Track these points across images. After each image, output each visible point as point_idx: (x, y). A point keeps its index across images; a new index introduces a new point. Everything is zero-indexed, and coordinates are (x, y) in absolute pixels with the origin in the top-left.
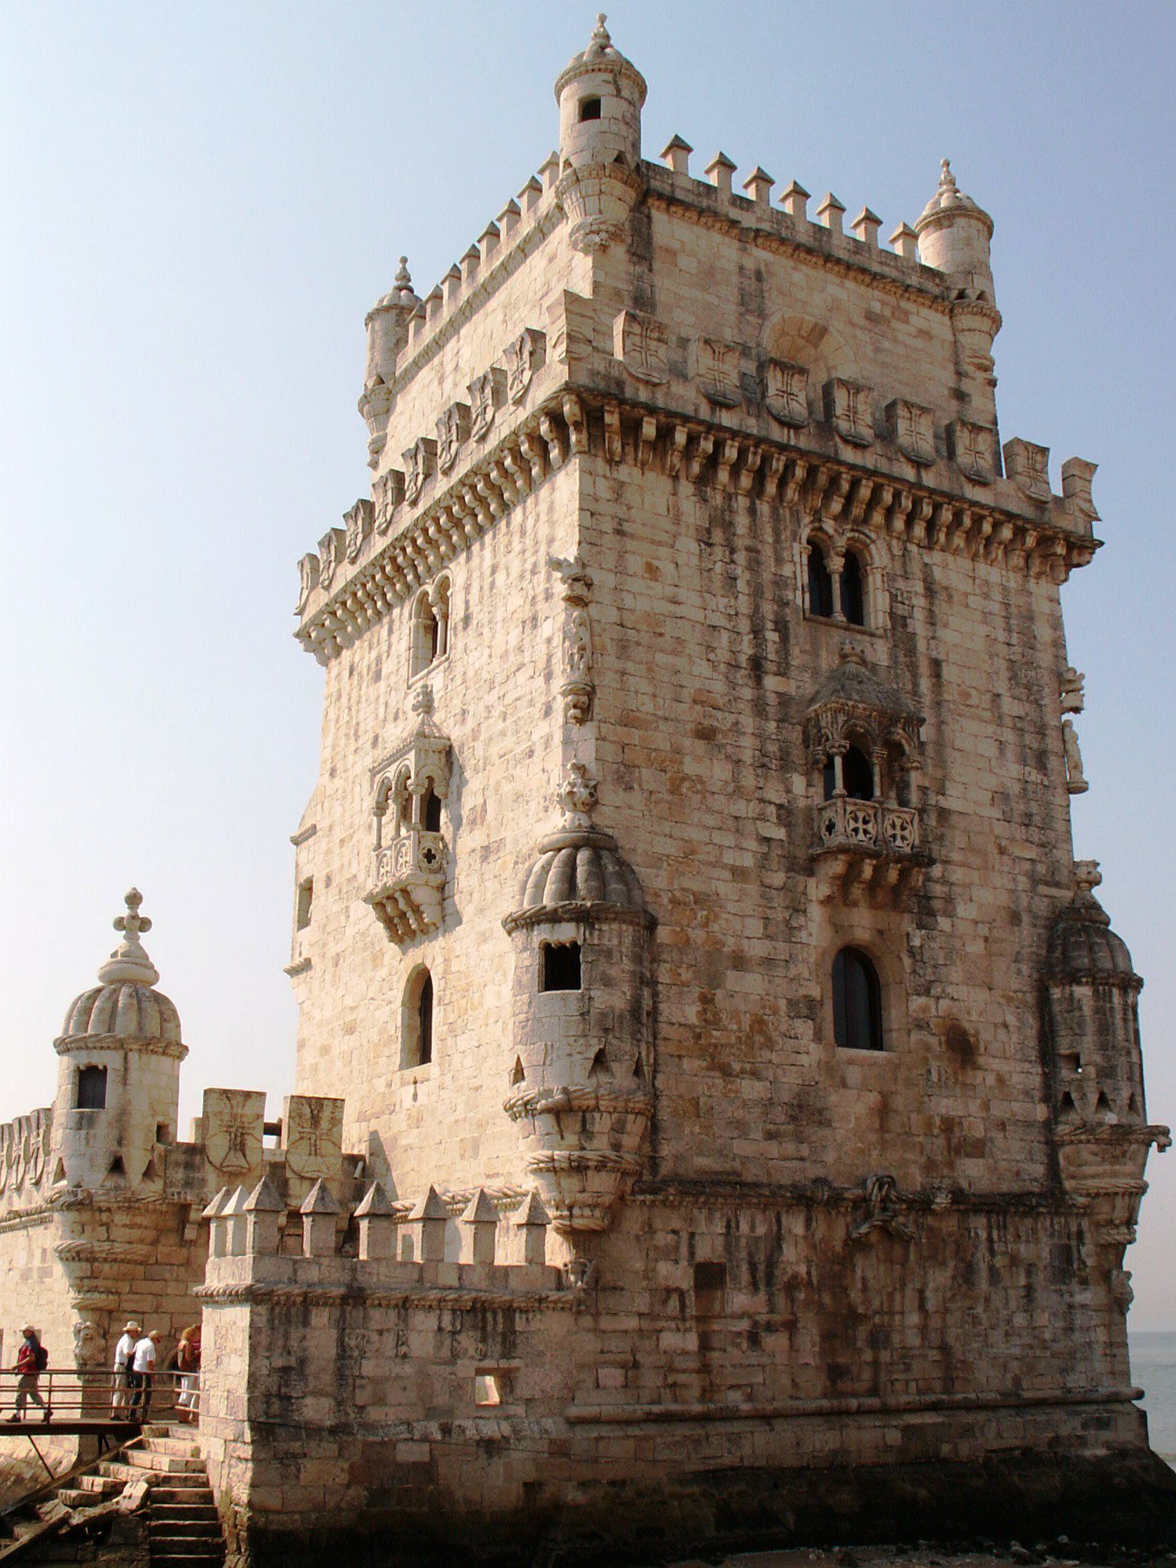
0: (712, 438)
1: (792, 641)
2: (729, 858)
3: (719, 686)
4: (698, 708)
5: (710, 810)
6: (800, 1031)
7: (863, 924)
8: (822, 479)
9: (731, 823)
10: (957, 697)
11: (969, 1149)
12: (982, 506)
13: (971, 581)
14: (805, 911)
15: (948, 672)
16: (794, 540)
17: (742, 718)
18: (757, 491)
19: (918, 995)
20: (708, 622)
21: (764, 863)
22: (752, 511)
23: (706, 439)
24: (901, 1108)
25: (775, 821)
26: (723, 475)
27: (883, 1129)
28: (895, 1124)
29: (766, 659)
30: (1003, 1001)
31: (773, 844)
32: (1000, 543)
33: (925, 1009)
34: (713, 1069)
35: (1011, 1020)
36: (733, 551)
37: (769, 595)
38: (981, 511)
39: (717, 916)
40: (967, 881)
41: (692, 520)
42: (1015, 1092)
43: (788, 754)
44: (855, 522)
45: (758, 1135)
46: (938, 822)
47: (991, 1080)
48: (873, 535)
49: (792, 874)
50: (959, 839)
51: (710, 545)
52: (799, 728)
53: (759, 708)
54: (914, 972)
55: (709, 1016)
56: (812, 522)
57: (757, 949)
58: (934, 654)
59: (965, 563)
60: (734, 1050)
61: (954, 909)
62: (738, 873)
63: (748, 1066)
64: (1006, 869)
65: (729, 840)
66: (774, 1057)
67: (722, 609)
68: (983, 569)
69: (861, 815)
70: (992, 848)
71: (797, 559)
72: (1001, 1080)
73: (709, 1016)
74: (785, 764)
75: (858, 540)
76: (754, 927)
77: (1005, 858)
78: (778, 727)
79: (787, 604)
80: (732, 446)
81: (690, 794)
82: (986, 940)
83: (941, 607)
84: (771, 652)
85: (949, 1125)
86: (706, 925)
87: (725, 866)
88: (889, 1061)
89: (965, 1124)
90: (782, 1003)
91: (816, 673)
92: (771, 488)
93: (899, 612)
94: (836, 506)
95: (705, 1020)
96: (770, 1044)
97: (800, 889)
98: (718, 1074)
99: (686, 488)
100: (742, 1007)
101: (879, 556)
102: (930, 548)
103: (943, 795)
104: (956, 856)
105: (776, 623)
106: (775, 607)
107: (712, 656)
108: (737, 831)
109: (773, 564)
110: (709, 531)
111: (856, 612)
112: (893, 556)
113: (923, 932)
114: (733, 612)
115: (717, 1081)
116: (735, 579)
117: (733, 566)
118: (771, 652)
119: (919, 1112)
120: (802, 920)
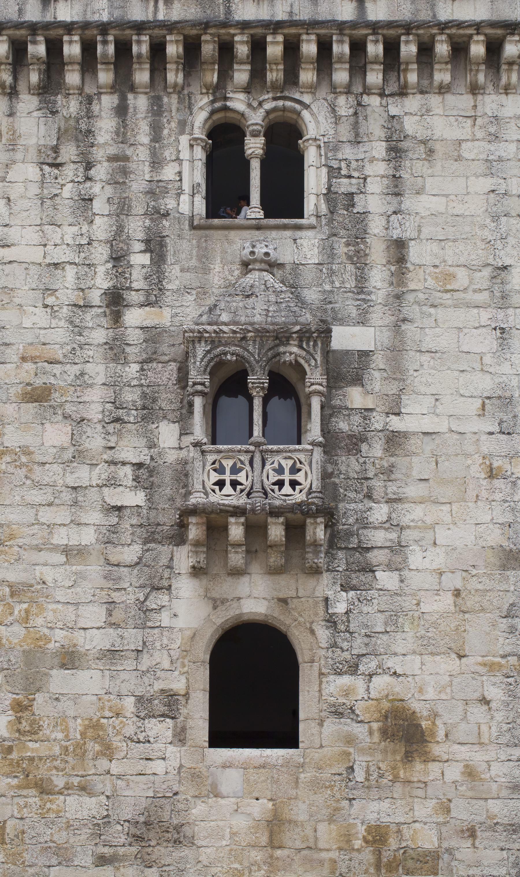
0: (41, 38)
1: (170, 259)
2: (61, 538)
3: (59, 335)
4: (29, 366)
5: (38, 485)
6: (151, 734)
7: (254, 598)
8: (209, 49)
9: (67, 496)
10: (431, 282)
11: (410, 864)
12: (460, 25)
13: (469, 122)
14: (169, 588)
15: (414, 253)
16: (182, 132)
17: (89, 368)
18: (124, 85)
19: (340, 674)
20: (48, 261)
21: (110, 538)
22: (121, 110)
23: (34, 42)
24: (302, 817)
25: (130, 483)
26: (73, 77)
27: (274, 844)
28: (293, 838)
29: (130, 289)
30: (482, 670)
31: (127, 512)
32: (511, 64)
33: (347, 692)
34: (27, 787)
35: (495, 693)
36: (89, 166)
37: (139, 208)
38: (461, 32)
39: (41, 609)
40: (429, 520)
41: (33, 141)
42: (494, 787)
43: (154, 400)
44: (274, 87)
45: (89, 861)
46: (386, 450)
47: (454, 772)
48: (307, 99)
49: (153, 545)
50: (418, 465)
51: (57, 166)
52: (173, 366)
53: (116, 351)
54: (334, 645)
55: (25, 725)
56: (213, 102)
57: (95, 641)
58: (396, 234)
59: (462, 101)
60: (57, 763)
61: (405, 560)
62: (72, 553)
63: (76, 781)
64: (498, 496)
65: (62, 515)
66: (115, 768)
67: (70, 241)
68: (491, 102)
69: (228, 464)
70: (477, 471)
71: (185, 155)
72: (470, 773)
73: (25, 725)
74: (149, 411)
75: (284, 109)
76: (94, 615)
77: (498, 483)
78: (142, 369)
79: (166, 215)
80: (70, 42)
81: (11, 469)
82: (457, 593)
83: (413, 167)
84: (138, 280)
85: (377, 836)
86: (27, 620)
87: (55, 548)
88: (287, 763)
89: (407, 832)
90: (129, 703)
91: (203, 291)
92: (142, 76)
93: (343, 190)
94: (241, 75)
95: (18, 731)
96: (108, 751)
97: (164, 561)
98: (33, 792)
99: (28, 102)
100: (71, 713)
101: (316, 123)
102: (402, 92)
103: (398, 414)
104: (412, 491)
105: (147, 242)
106: (148, 222)
107: (50, 300)
108: (75, 503)
109: (147, 169)
110: (56, 149)
111: (285, 201)
112: (337, 119)
113: (352, 593)
114: (84, 241)
115: (30, 800)
116: (91, 200)
117: (88, 184)
118: (138, 280)
119: (331, 820)
120: (163, 598)
